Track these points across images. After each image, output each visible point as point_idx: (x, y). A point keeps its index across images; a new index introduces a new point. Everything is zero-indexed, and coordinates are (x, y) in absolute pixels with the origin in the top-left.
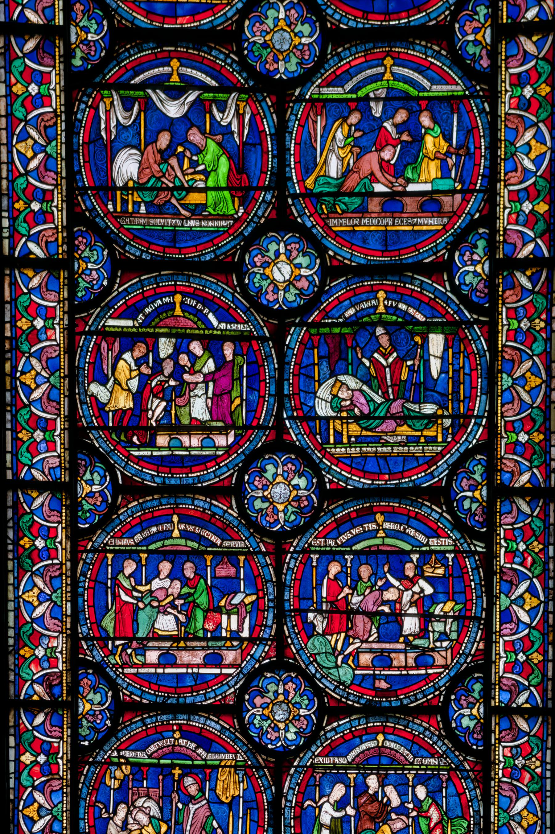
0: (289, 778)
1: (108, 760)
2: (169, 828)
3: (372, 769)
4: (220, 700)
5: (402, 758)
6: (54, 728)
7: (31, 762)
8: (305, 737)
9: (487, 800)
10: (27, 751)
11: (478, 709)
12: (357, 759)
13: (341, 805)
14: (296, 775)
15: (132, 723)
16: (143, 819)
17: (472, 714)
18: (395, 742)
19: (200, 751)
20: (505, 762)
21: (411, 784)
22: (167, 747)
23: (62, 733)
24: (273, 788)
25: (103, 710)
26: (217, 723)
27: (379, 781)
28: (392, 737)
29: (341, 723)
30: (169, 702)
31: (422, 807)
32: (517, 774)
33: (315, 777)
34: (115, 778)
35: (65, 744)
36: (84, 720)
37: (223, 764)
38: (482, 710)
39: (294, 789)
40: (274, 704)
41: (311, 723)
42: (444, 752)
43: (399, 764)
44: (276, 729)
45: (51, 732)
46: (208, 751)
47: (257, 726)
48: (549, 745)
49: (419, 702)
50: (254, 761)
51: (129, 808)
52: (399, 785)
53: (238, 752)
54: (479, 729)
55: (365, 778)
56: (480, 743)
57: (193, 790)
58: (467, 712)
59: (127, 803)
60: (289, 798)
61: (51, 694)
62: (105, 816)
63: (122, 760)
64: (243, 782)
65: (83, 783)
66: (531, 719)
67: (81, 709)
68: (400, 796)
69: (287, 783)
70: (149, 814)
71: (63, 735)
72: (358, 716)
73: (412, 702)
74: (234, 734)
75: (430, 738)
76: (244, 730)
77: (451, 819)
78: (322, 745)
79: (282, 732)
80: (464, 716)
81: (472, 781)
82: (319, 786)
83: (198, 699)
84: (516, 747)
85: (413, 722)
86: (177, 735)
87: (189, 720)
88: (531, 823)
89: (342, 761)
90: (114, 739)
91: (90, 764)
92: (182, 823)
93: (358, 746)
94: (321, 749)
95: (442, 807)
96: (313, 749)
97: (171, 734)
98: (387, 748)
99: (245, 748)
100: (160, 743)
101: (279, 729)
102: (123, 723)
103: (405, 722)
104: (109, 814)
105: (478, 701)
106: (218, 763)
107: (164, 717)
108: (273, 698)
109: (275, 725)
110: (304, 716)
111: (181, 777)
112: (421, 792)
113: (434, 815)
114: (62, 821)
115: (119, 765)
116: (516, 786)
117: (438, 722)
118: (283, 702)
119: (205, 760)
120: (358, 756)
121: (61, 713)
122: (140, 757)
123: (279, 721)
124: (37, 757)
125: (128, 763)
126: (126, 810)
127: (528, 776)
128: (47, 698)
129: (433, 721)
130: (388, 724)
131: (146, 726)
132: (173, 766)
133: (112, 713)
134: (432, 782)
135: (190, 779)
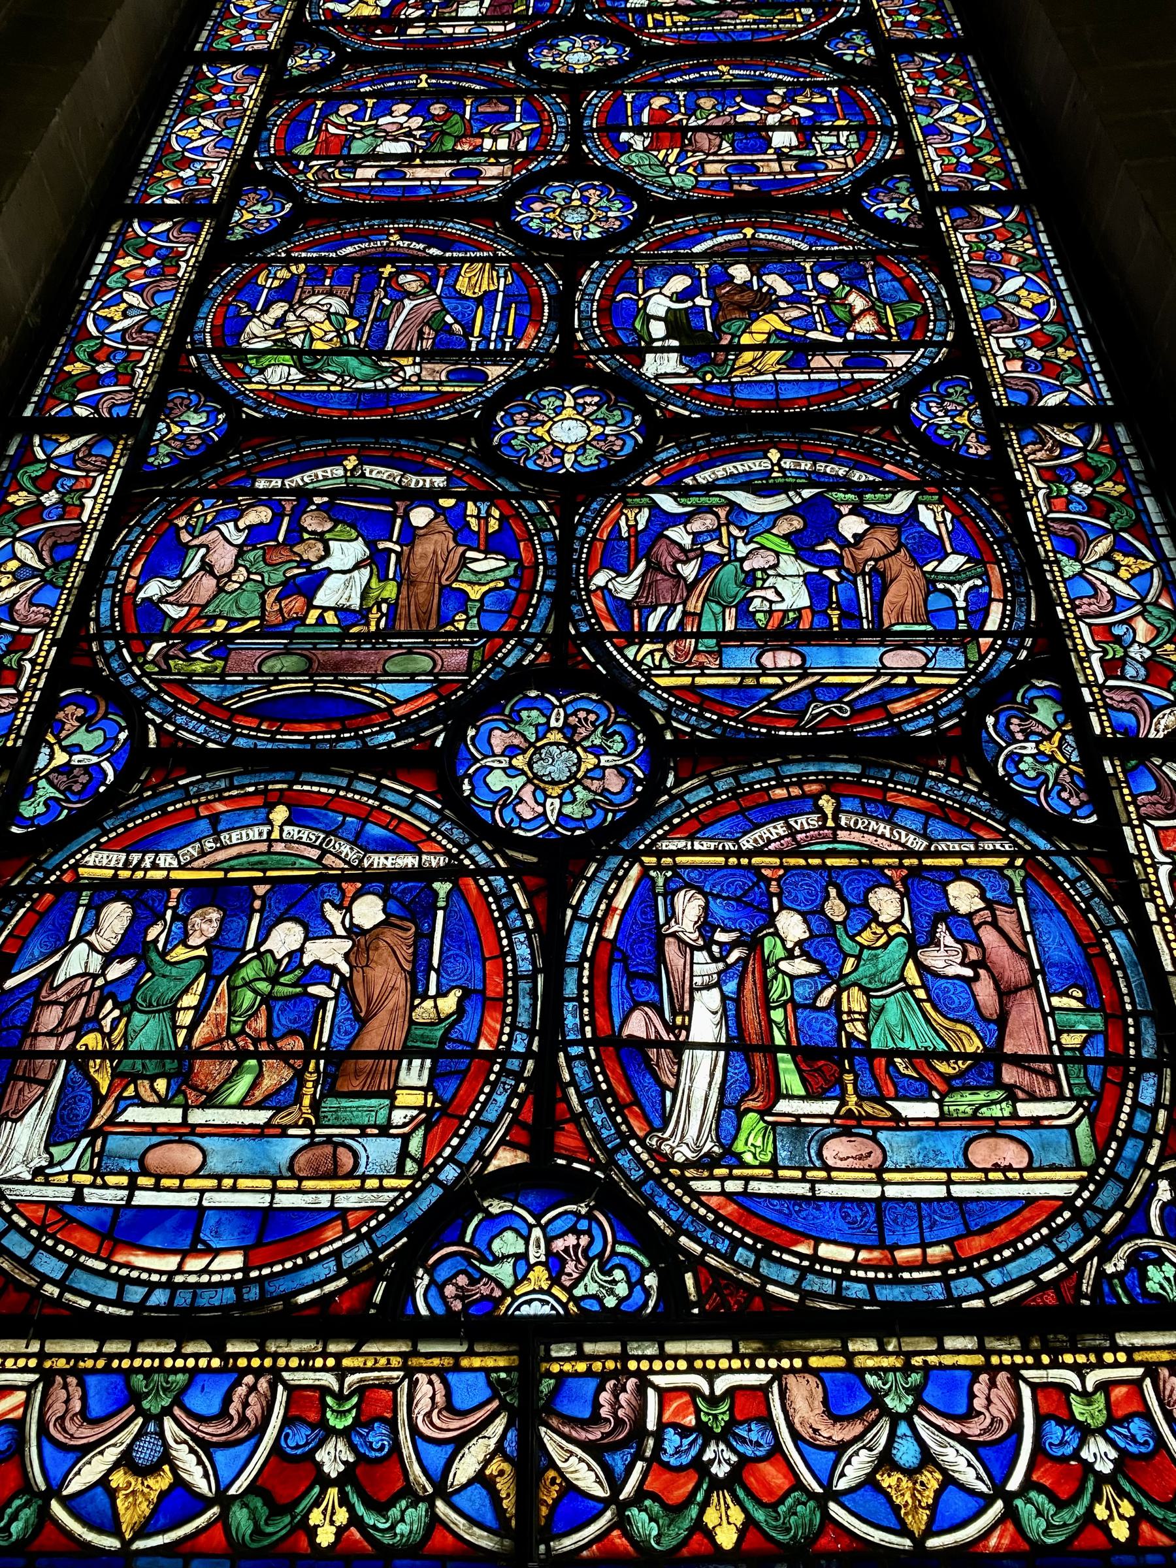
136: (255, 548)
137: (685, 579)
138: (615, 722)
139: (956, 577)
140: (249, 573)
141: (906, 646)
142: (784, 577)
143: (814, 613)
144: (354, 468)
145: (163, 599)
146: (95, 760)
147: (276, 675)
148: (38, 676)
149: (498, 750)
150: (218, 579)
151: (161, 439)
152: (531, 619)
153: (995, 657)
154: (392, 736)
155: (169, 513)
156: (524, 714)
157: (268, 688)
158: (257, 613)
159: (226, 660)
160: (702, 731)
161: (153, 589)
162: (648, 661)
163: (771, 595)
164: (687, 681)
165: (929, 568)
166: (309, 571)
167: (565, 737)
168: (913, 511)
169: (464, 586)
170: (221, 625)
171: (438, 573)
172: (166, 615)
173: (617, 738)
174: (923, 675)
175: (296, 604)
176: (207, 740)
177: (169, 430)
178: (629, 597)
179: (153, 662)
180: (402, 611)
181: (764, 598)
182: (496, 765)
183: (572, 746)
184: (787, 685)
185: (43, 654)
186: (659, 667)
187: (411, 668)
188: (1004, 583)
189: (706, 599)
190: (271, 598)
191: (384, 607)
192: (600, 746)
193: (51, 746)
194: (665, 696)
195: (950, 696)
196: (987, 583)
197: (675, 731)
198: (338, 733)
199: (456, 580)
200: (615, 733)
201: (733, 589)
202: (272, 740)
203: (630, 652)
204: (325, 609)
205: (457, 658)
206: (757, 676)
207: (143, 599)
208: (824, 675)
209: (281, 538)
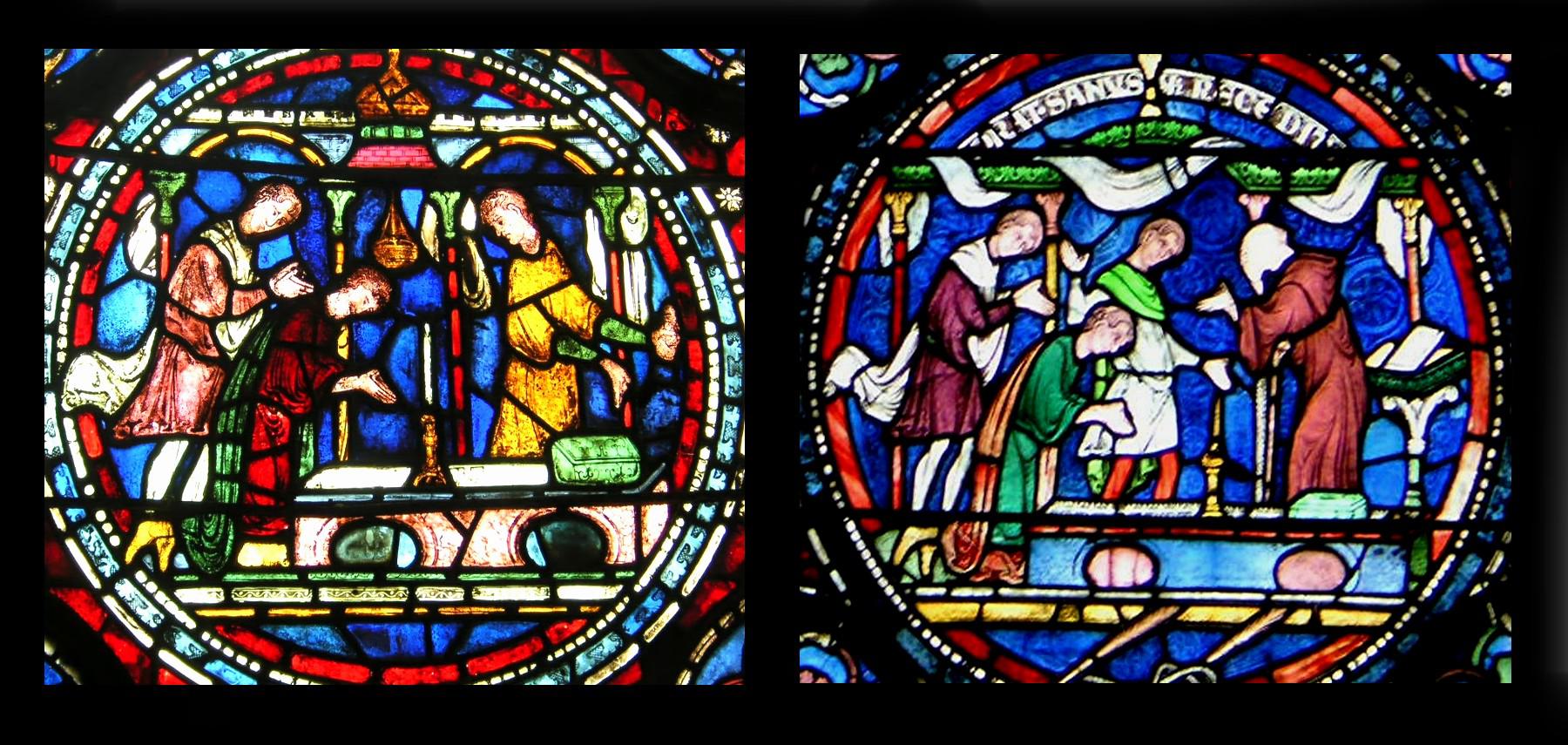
137: (980, 373)
139: (1415, 384)
142: (1140, 375)
143: (1183, 463)
153: (1455, 565)
165: (1374, 361)
168: (1368, 214)
174: (1336, 605)
188: (1493, 394)
195: (1372, 651)
201: (1055, 401)
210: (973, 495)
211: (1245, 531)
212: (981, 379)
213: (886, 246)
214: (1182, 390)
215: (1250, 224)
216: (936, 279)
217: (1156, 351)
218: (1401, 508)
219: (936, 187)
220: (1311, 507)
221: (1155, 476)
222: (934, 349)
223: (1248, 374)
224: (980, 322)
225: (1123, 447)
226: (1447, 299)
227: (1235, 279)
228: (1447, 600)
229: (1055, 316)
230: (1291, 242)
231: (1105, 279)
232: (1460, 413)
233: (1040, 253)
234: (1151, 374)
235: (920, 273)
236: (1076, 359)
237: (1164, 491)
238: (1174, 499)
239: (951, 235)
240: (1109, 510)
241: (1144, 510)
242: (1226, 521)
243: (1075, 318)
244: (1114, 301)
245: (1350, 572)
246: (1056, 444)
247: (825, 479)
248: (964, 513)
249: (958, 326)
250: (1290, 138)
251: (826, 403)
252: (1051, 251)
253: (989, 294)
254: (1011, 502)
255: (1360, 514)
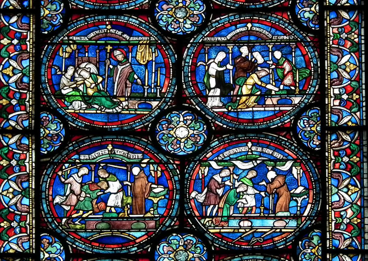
0: (187, 50)
1: (61, 42)
2: (104, 79)
3: (244, 43)
4: (138, 7)
5: (265, 36)
6: (24, 25)
7: (8, 44)
8: (197, 27)
9: (322, 57)
10: (5, 37)
11: (315, 7)
12: (233, 38)
13: (222, 64)
14: (191, 48)
15: (77, 21)
16: (85, 74)
17: (311, 10)
18: (259, 28)
19: (125, 36)
20: (334, 36)
21: (270, 50)
22: (102, 34)
23: (30, 27)
24: (176, 56)
25: (58, 14)
26: (137, 20)
27: (248, 50)
28: (257, 25)
29: (222, 18)
30: (103, 8)
31: (278, 63)
32: (342, 43)
33: (205, 49)
34: (66, 52)
35: (31, 34)
36: (44, 20)
37: (141, 42)
38: (317, 8)
39: (190, 56)
40: (176, 9)
41: (201, 19)
42: (293, 32)
43: (262, 40)
44: (177, 22)
45: (21, 27)
46: (130, 36)
47: (165, 21)
48: (363, 25)
49: (275, 5)
50: (163, 41)
51: (75, 69)
52: (263, 51)
53: (151, 36)
54: (316, 18)
55: (239, 48)
56: (317, 26)
57: (120, 58)
58: (308, 9)
59: (74, 66)
60: (187, 60)
61: (22, 5)
62: (59, 73)
63: (71, 42)
64: (155, 52)
65: (44, 55)
66: (350, 12)
67: (42, 14)
68: (263, 57)
69: (186, 52)
70: (90, 72)
71: (30, 28)
72: (234, 14)
73: (270, 5)
74: (148, 26)
75: (283, 25)
76: (155, 23)
77: (298, 69)
78: (209, 30)
79: (182, 24)
80: (306, 11)
81: (312, 47)
82: (208, 53)
83: (124, 6)
84: (341, 27)
85: (271, 16)
86: (109, 27)
87: (117, 18)
88: (352, 69)
89: (223, 39)
90: (65, 30)
91: (49, 44)
92: (113, 77)
93: (234, 30)
94: (208, 33)
95: (292, 62)
96: (203, 33)
97: (105, 26)
98: (254, 31)
99: (156, 34)
100: (97, 32)
101: (180, 22)
102: (72, 20)
103: (266, 16)
104: (62, 72)
105: (315, 3)
106: (137, 42)
107: (100, 17)
108: (175, 5)
109: (177, 20)
110: (197, 15)
111: (112, 51)
112: (278, 54)
113: (287, 67)
114: (29, 77)
115: (69, 45)
116: (341, 49)
117: (289, 16)
118: (182, 7)
119: (129, 41)
120: (234, 36)
121: (28, 16)
122: (84, 39)
123: (180, 18)
124: (12, 41)
125: (75, 43)
126: (73, 70)
127: (349, 43)
128: (19, 7)
129: (284, 15)
130: (254, 18)
131: (87, 22)
132: (107, 44)
133: (64, 15)
134: (285, 50)
135: (118, 51)
136: (86, 184)
137: (219, 195)
138: (198, 244)
139: (299, 195)
140: (86, 194)
141: (281, 220)
142: (248, 195)
143: (256, 208)
144: (111, 151)
145: (62, 204)
146: (56, 256)
147: (101, 230)
148: (32, 229)
149: (166, 252)
150: (77, 196)
151: (43, 136)
152: (173, 209)
154: (136, 248)
155: (55, 169)
156: (172, 241)
157: (99, 234)
158: (91, 208)
159: (85, 224)
160: (222, 246)
161: (58, 200)
162: (207, 224)
163: (244, 201)
164: (218, 231)
165: (292, 192)
166: (104, 193)
167: (184, 248)
169: (152, 198)
170: (81, 212)
171: (143, 193)
172: (64, 209)
173: (199, 248)
175: (102, 205)
176: (86, 250)
177: (45, 132)
178: (202, 202)
179: (64, 225)
180: (134, 207)
181: (242, 203)
182: (165, 257)
183: (186, 250)
184: (246, 232)
185: (31, 222)
186: (210, 226)
187: (139, 227)
188: (313, 196)
189: (225, 203)
190: (94, 203)
191: (129, 206)
192: (194, 251)
193: (43, 252)
194: (212, 235)
196: (308, 197)
197: (215, 247)
198: (121, 248)
199: (149, 196)
200: (198, 247)
201: (233, 199)
202: (103, 250)
203: (202, 221)
204: (111, 207)
205: (152, 224)
206: (238, 229)
207: (56, 203)
208: (257, 229)
209: (93, 180)
210: (218, 213)
211: (268, 218)
212: (219, 195)
213: (200, 175)
214: (256, 197)
215: (269, 171)
216: (210, 180)
217: (251, 191)
218: (296, 214)
219: (210, 166)
220: (280, 214)
221: (252, 210)
222: (210, 191)
223: (268, 195)
224: (219, 187)
225: (245, 206)
226: (305, 182)
227: (266, 179)
228: (304, 227)
229: (233, 186)
230: (276, 174)
231: (242, 180)
232: (307, 199)
233: (230, 176)
234: (251, 194)
235: (207, 179)
236: (237, 192)
237: (253, 212)
238: (255, 213)
239: (213, 173)
240: (243, 215)
241: (250, 215)
242: (265, 217)
243: (236, 186)
244: (243, 183)
245: (287, 224)
246: (233, 205)
247: (191, 211)
248: (216, 216)
249: (215, 187)
250: (275, 157)
251: (190, 200)
252: (232, 176)
253: (220, 183)
254: (225, 214)
255: (289, 215)
